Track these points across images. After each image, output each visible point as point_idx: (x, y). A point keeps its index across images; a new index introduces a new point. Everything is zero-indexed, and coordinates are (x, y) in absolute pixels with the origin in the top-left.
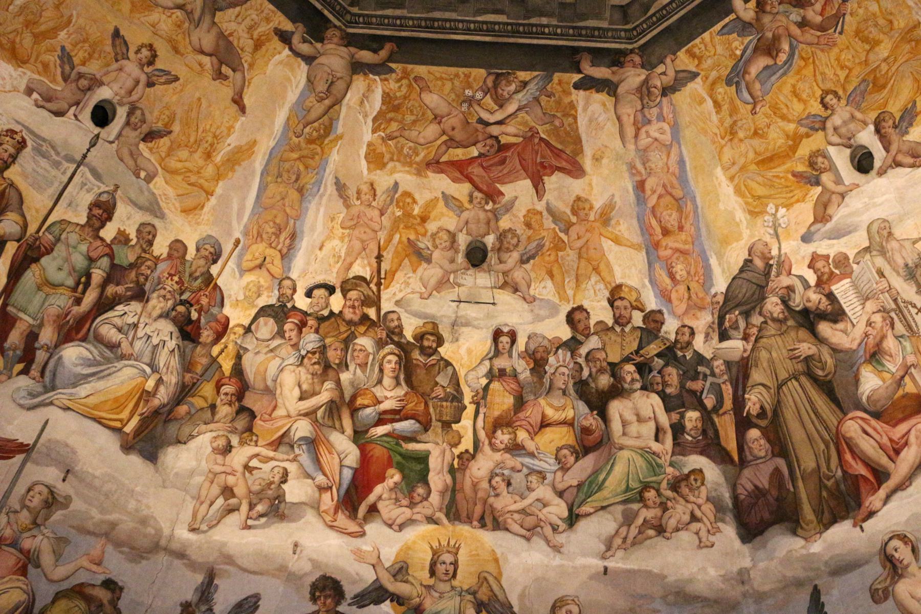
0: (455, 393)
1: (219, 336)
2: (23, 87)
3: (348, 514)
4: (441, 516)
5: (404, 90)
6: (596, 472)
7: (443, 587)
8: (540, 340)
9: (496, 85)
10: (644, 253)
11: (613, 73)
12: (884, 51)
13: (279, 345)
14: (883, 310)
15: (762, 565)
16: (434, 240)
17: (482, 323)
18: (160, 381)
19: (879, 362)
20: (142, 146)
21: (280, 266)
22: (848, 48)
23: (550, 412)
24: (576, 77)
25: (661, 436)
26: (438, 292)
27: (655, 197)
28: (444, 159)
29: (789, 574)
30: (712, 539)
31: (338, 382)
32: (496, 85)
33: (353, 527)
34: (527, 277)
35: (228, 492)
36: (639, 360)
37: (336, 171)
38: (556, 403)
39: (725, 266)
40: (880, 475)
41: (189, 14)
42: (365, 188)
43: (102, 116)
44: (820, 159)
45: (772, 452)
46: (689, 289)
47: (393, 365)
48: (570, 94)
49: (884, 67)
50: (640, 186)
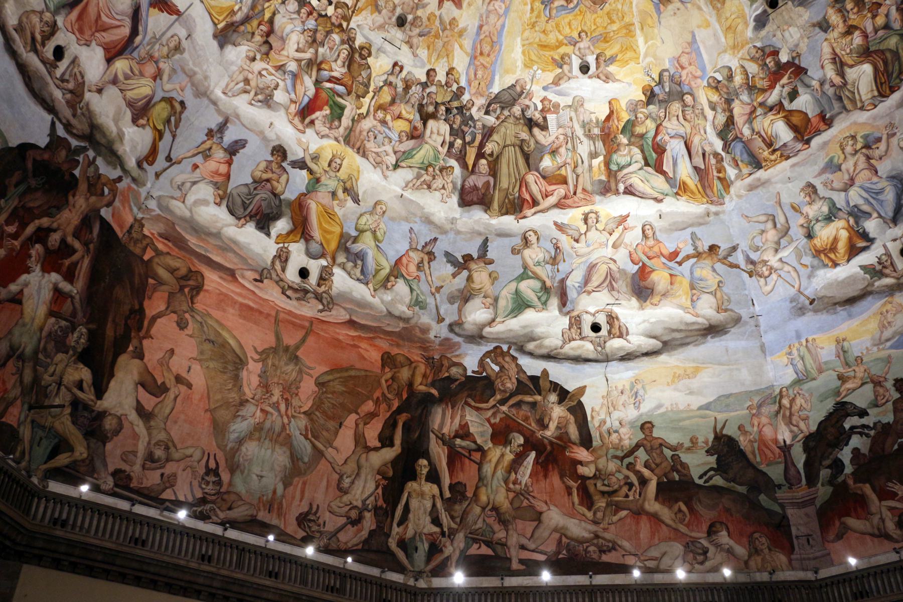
4: (341, 139)
6: (413, 149)
7: (332, 174)
12: (615, 27)
14: (566, 135)
18: (240, 8)
23: (404, 112)
29: (477, 228)
31: (317, 51)
33: (300, 127)
35: (247, 81)
40: (535, 203)
49: (612, 34)
50: (481, 27)
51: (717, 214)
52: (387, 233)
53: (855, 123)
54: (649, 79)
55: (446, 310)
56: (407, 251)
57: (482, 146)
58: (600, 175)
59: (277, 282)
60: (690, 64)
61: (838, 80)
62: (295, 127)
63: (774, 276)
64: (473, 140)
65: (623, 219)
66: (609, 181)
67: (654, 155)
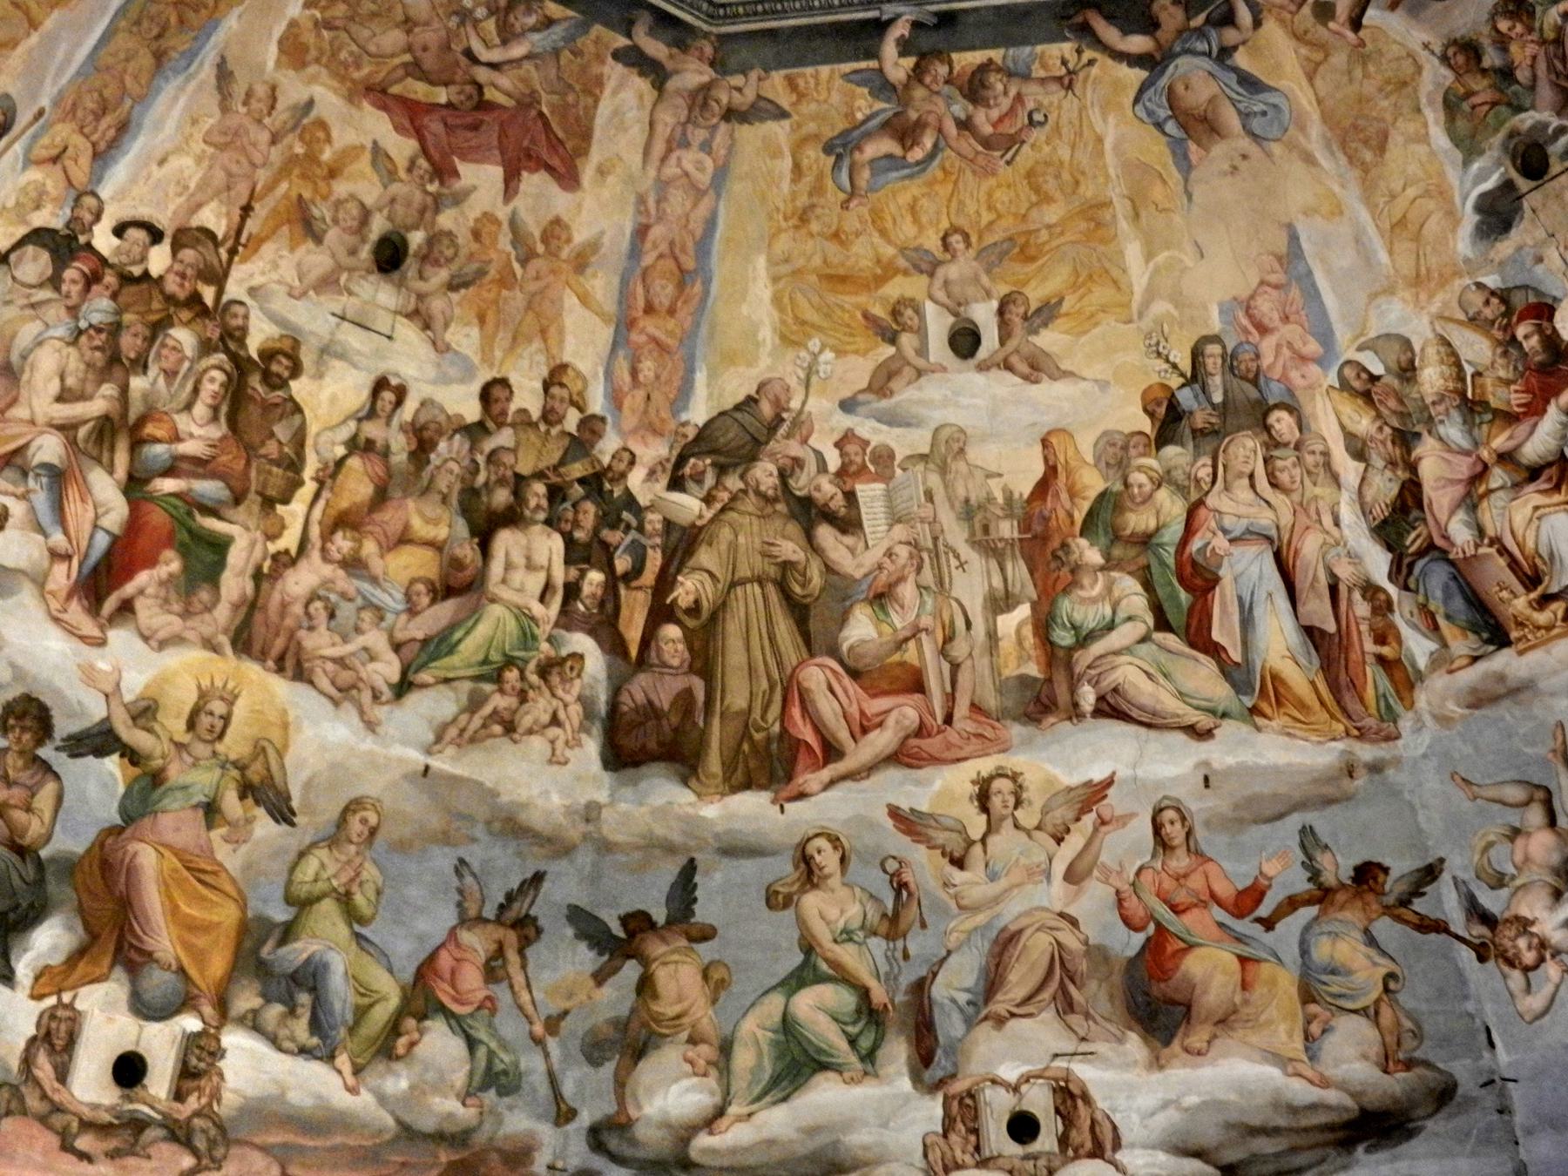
0: (293, 456)
3: (86, 603)
4: (224, 640)
6: (452, 627)
7: (201, 750)
8: (437, 412)
10: (612, 330)
11: (671, 56)
12: (1052, 214)
13: (48, 301)
15: (623, 806)
16: (337, 211)
17: (364, 362)
19: (883, 608)
21: (87, 169)
22: (1009, 186)
23: (417, 524)
24: (622, 41)
25: (548, 596)
26: (317, 294)
27: (654, 254)
28: (395, 89)
29: (660, 831)
30: (568, 753)
31: (124, 390)
33: (89, 627)
34: (448, 312)
36: (554, 479)
37: (227, 45)
39: (716, 392)
40: (831, 752)
42: (261, 91)
44: (909, 312)
45: (691, 666)
46: (649, 398)
47: (215, 387)
48: (603, 62)
49: (1044, 235)
50: (641, 232)
51: (1376, 768)
52: (387, 891)
54: (1161, 365)
55: (580, 1084)
56: (452, 933)
57: (665, 582)
58: (1022, 660)
59: (43, 1120)
60: (1286, 319)
62: (71, 631)
63: (1552, 970)
64: (637, 570)
65: (1096, 793)
66: (1049, 680)
67: (1184, 596)
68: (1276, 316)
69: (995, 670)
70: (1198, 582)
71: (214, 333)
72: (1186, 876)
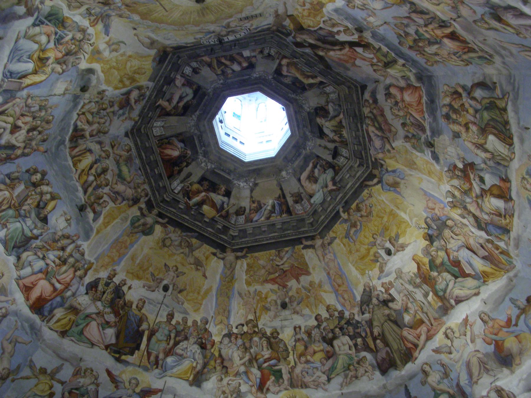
1: (213, 346)
2: (142, 286)
5: (252, 261)
6: (333, 364)
9: (279, 254)
12: (385, 219)
14: (406, 295)
15: (389, 382)
18: (197, 363)
20: (179, 295)
23: (316, 348)
28: (268, 278)
30: (373, 377)
31: (250, 353)
32: (279, 254)
35: (224, 392)
36: (339, 326)
38: (317, 345)
41: (185, 254)
42: (247, 293)
43: (166, 289)
44: (377, 254)
49: (387, 224)
50: (328, 274)
51: (516, 276)
53: (517, 170)
54: (422, 230)
58: (437, 304)
61: (488, 155)
64: (366, 334)
65: (466, 320)
66: (444, 304)
67: (456, 269)
68: (433, 205)
69: (433, 309)
70: (457, 264)
71: (260, 335)
72: (493, 326)
